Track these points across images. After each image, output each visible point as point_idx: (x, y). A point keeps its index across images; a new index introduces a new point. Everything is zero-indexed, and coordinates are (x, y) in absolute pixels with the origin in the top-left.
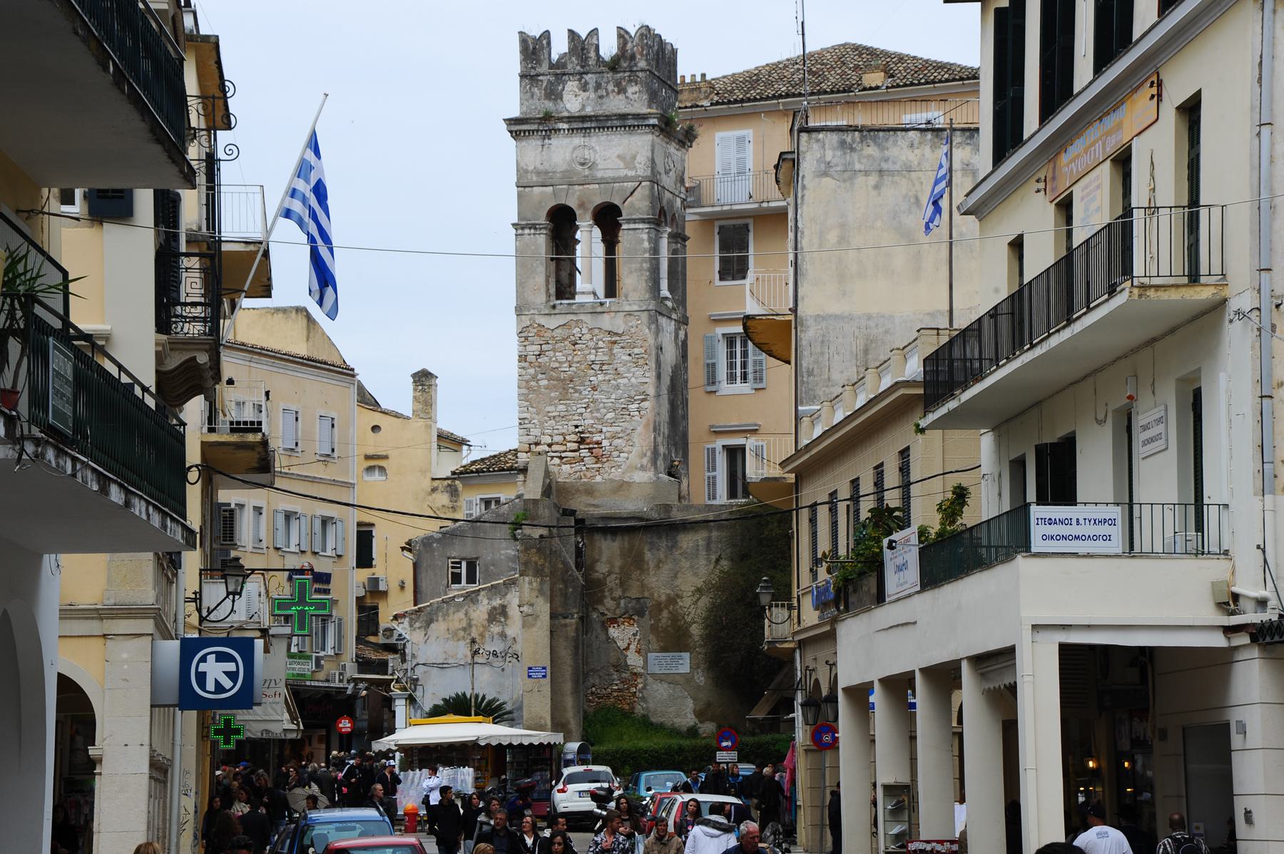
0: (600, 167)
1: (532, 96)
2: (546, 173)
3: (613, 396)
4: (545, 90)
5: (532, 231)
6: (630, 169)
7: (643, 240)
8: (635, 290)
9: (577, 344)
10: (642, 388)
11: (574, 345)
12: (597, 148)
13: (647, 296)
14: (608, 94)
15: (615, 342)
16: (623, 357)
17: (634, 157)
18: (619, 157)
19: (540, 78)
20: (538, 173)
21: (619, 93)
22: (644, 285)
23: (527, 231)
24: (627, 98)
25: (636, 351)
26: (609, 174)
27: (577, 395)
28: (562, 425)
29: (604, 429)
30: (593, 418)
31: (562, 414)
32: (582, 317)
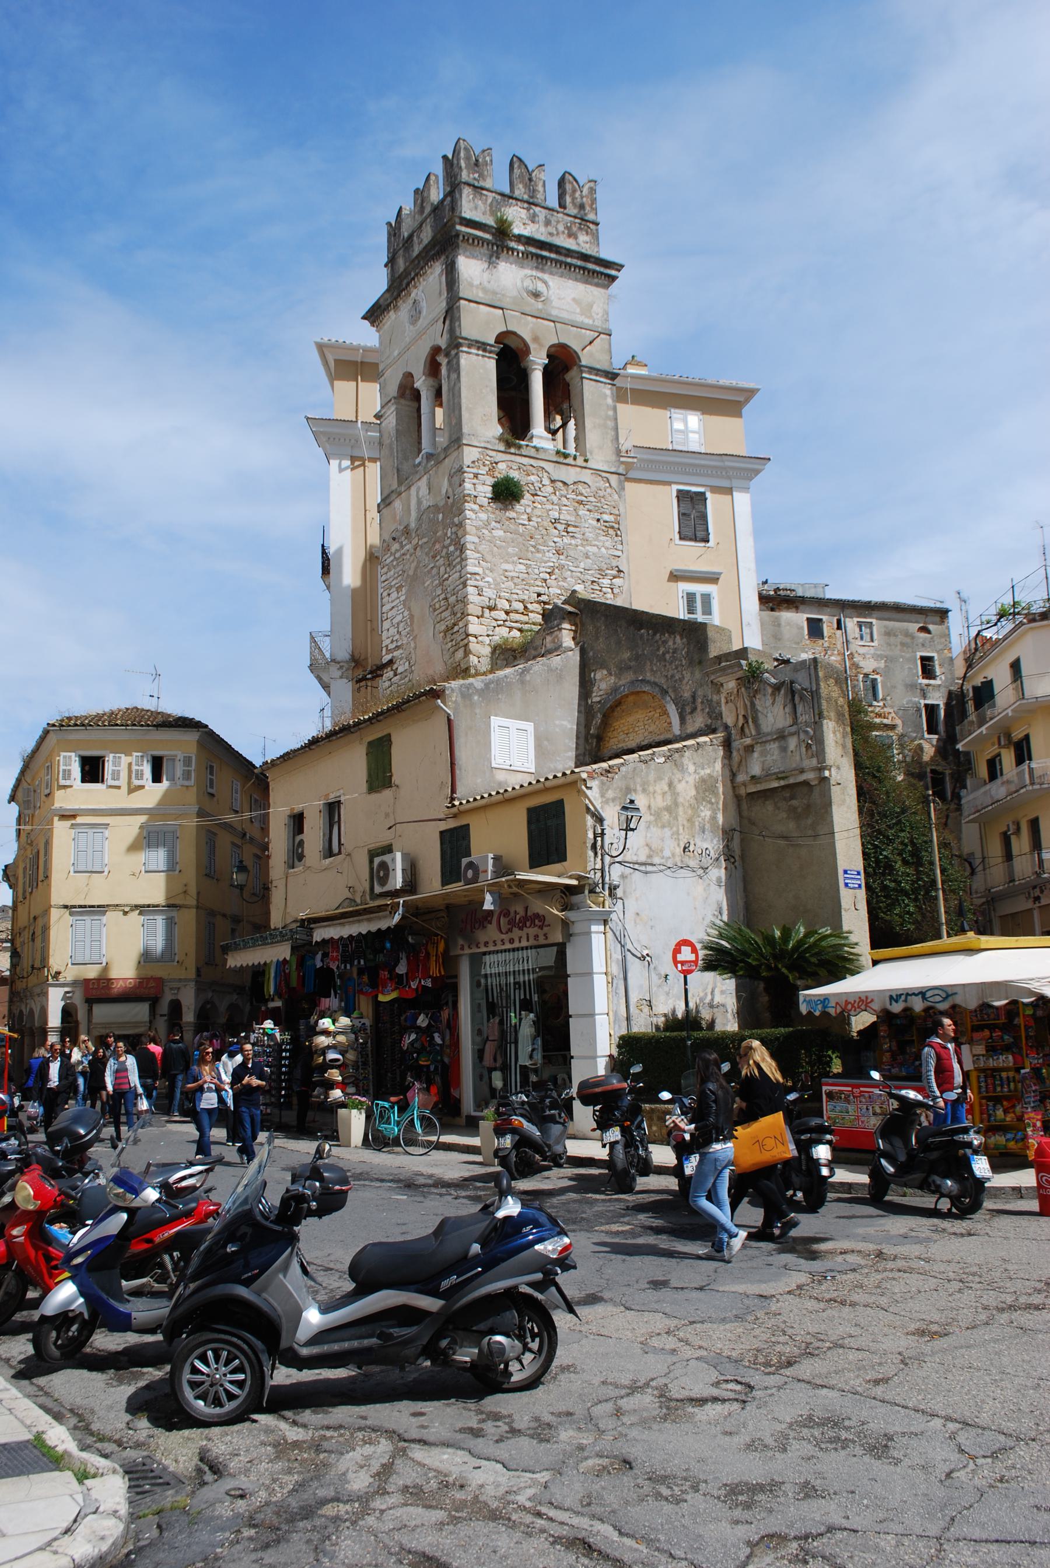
2: (495, 293)
4: (491, 205)
5: (480, 352)
6: (587, 317)
7: (606, 396)
9: (536, 495)
10: (614, 563)
11: (533, 495)
12: (550, 283)
14: (558, 234)
16: (590, 521)
17: (590, 306)
18: (574, 300)
19: (484, 192)
20: (485, 290)
22: (610, 444)
23: (474, 351)
24: (578, 244)
25: (606, 517)
26: (564, 315)
28: (523, 590)
30: (560, 588)
31: (521, 575)
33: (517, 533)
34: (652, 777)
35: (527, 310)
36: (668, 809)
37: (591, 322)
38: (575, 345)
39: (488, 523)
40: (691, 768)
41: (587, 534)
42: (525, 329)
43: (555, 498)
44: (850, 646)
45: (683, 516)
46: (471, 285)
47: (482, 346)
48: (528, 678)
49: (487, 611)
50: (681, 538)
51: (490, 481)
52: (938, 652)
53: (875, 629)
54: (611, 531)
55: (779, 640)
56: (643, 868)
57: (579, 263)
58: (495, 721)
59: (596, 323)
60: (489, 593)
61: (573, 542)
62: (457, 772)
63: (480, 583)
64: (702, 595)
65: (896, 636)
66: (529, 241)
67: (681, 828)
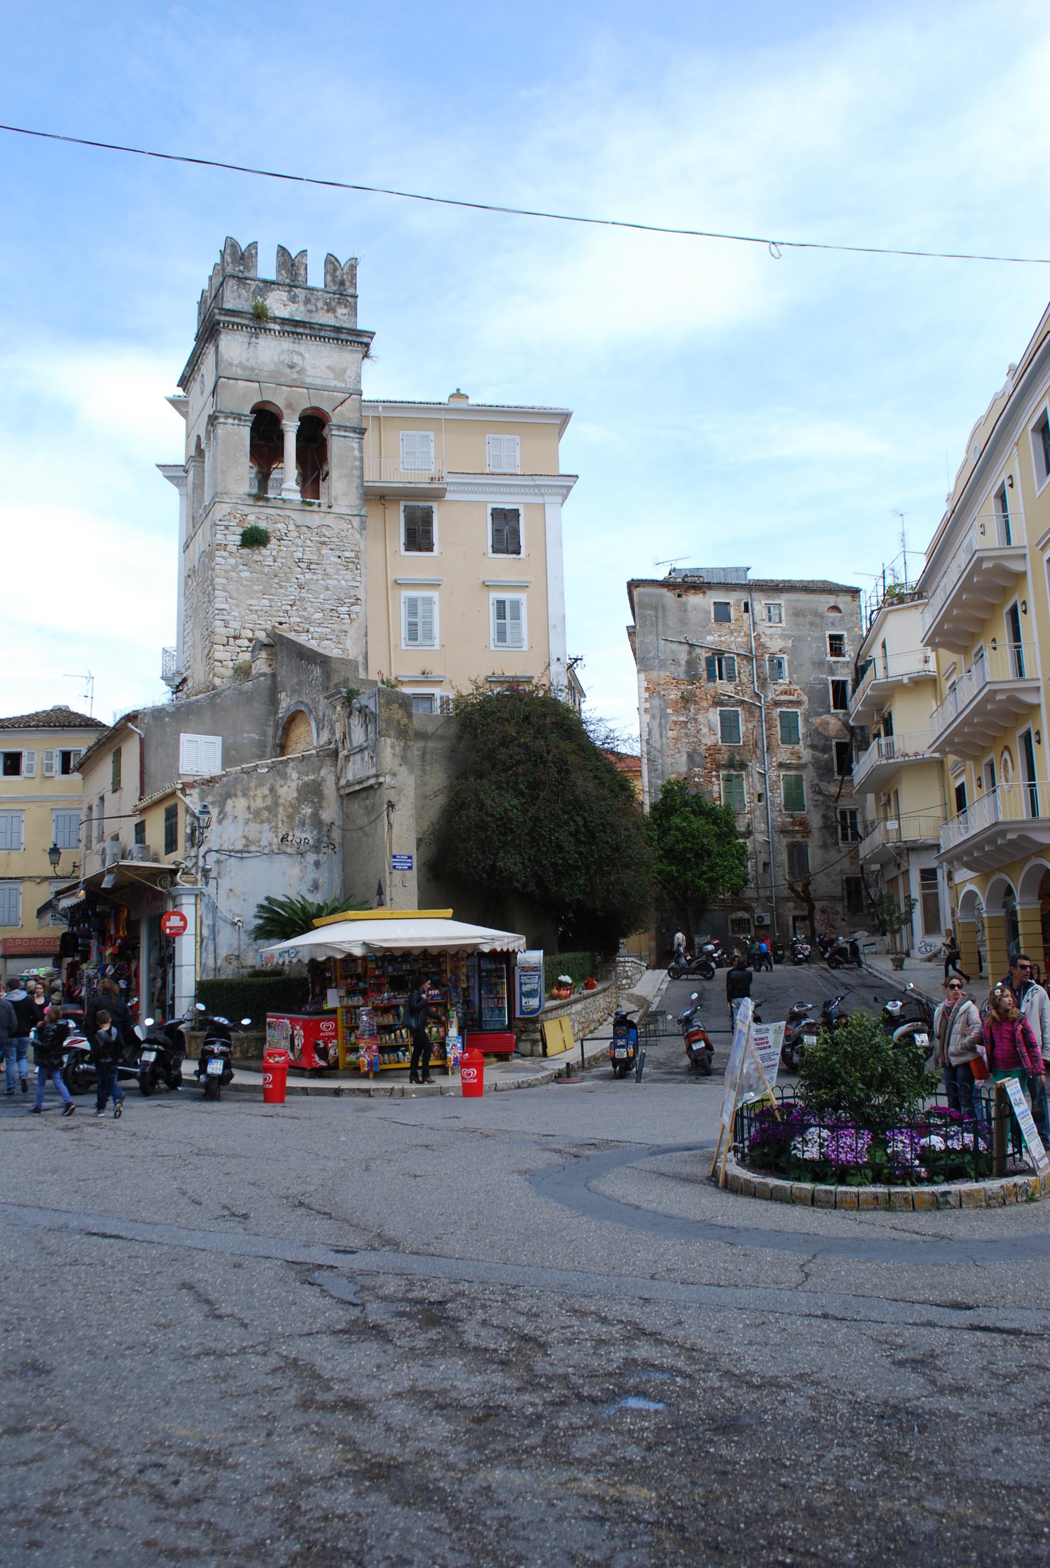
0: (308, 373)
1: (239, 297)
2: (252, 369)
3: (322, 596)
5: (236, 422)
6: (341, 381)
8: (345, 495)
12: (306, 356)
13: (358, 502)
14: (317, 310)
15: (324, 543)
17: (344, 371)
18: (328, 367)
19: (248, 282)
20: (244, 368)
21: (328, 311)
22: (355, 491)
23: (230, 421)
24: (336, 317)
25: (347, 554)
26: (318, 382)
27: (282, 591)
29: (312, 629)
30: (300, 617)
31: (265, 609)
32: (288, 513)
33: (262, 572)
34: (253, 784)
35: (282, 380)
36: (268, 809)
37: (343, 385)
38: (326, 407)
39: (234, 568)
40: (295, 776)
41: (328, 570)
42: (279, 399)
43: (299, 542)
44: (757, 627)
45: (497, 532)
46: (231, 364)
47: (238, 417)
48: (218, 701)
49: (231, 640)
50: (494, 552)
51: (240, 530)
52: (847, 630)
53: (783, 610)
54: (351, 566)
55: (686, 624)
56: (239, 855)
57: (332, 335)
58: (184, 737)
59: (348, 386)
60: (234, 624)
61: (315, 577)
62: (146, 779)
63: (227, 617)
64: (511, 602)
65: (804, 616)
66: (284, 321)
67: (280, 824)
